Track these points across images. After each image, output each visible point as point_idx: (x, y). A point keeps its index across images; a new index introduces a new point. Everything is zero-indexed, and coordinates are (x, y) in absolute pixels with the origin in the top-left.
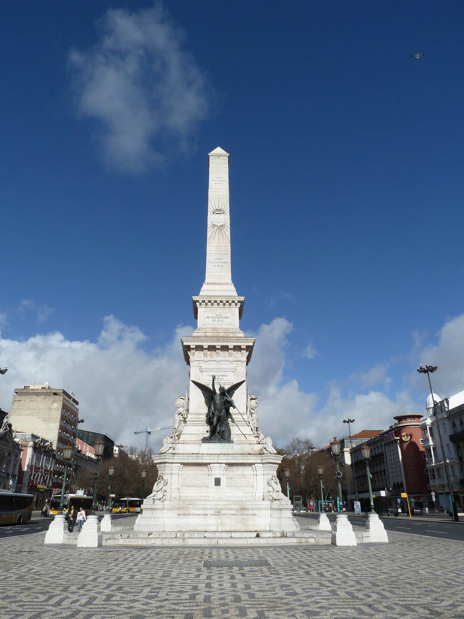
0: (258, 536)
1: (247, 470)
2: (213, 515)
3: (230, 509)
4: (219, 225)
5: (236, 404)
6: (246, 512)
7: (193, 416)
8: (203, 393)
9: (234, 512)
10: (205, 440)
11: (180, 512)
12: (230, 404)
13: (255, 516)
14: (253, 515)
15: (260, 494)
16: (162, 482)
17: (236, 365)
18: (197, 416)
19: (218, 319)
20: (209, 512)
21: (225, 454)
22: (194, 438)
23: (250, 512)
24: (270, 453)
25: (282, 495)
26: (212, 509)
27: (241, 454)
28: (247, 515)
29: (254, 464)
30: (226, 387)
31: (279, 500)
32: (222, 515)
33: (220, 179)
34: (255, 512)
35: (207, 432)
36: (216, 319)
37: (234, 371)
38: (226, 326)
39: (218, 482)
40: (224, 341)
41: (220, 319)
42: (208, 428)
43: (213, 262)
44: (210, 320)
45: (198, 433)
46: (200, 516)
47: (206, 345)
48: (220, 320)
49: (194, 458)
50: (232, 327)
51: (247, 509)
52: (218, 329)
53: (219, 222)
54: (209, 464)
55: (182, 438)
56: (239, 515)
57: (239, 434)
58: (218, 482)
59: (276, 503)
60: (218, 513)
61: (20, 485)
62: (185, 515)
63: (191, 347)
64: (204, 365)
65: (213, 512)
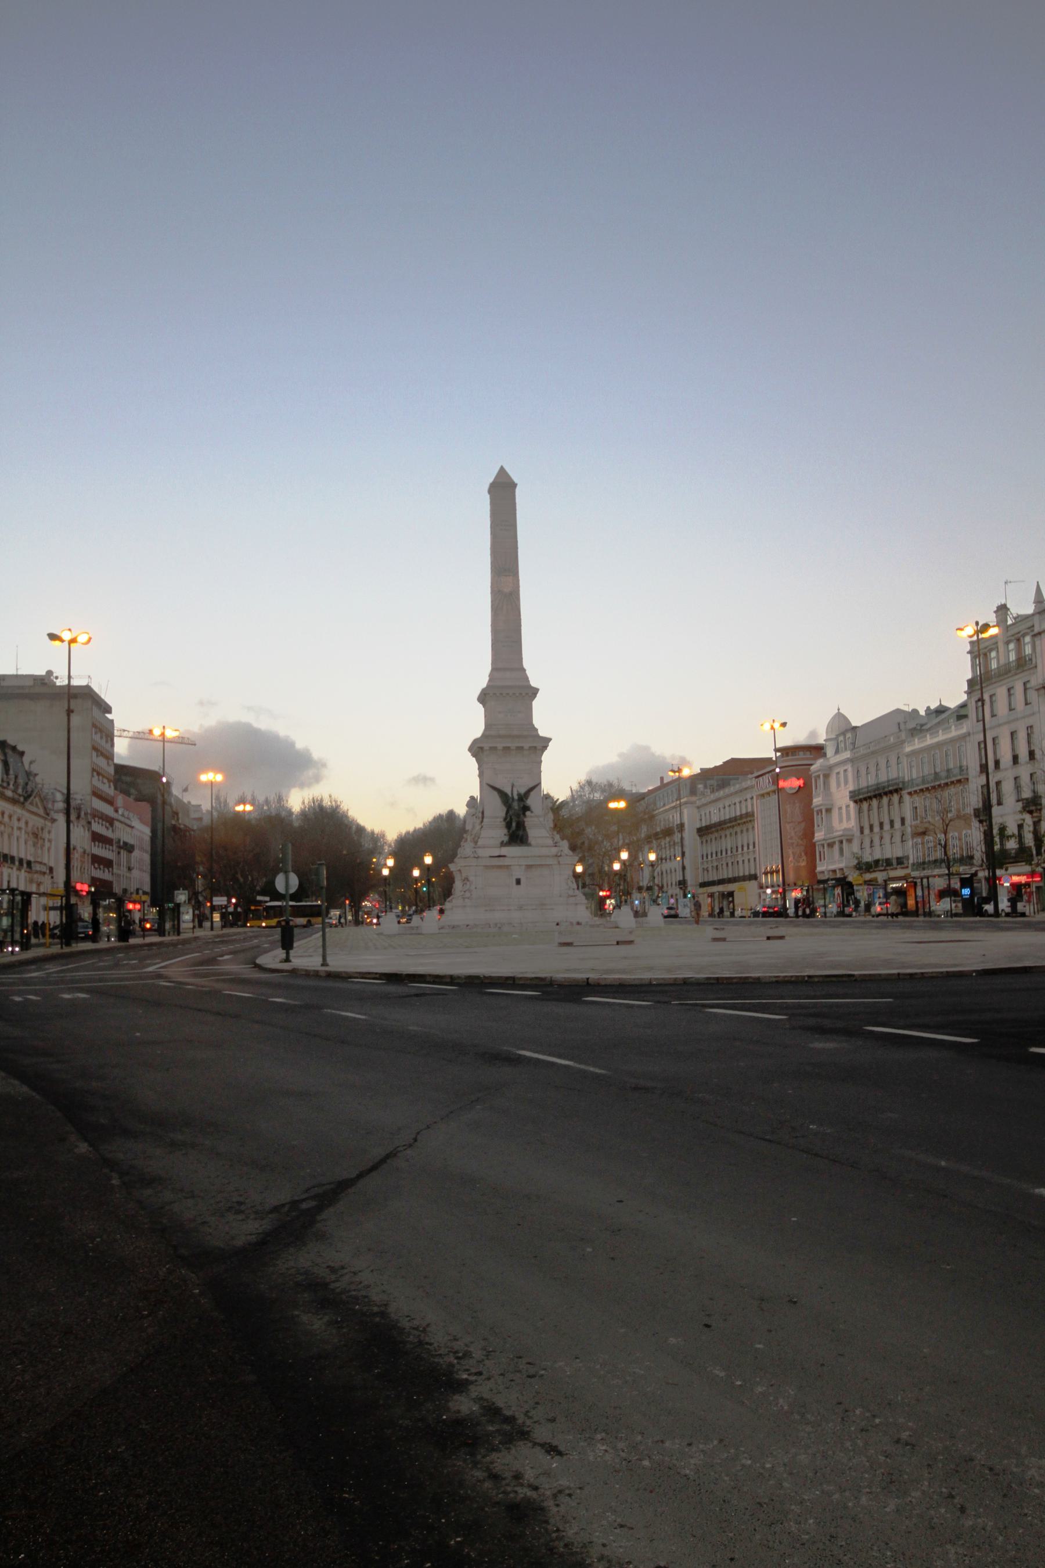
0: (558, 924)
4: (507, 590)
5: (533, 807)
8: (498, 793)
10: (503, 844)
12: (526, 809)
16: (468, 883)
21: (524, 857)
24: (567, 855)
25: (577, 892)
30: (523, 791)
35: (505, 835)
39: (518, 882)
42: (505, 831)
47: (500, 746)
55: (480, 843)
58: (518, 882)
59: (572, 900)
60: (520, 908)
63: (485, 748)
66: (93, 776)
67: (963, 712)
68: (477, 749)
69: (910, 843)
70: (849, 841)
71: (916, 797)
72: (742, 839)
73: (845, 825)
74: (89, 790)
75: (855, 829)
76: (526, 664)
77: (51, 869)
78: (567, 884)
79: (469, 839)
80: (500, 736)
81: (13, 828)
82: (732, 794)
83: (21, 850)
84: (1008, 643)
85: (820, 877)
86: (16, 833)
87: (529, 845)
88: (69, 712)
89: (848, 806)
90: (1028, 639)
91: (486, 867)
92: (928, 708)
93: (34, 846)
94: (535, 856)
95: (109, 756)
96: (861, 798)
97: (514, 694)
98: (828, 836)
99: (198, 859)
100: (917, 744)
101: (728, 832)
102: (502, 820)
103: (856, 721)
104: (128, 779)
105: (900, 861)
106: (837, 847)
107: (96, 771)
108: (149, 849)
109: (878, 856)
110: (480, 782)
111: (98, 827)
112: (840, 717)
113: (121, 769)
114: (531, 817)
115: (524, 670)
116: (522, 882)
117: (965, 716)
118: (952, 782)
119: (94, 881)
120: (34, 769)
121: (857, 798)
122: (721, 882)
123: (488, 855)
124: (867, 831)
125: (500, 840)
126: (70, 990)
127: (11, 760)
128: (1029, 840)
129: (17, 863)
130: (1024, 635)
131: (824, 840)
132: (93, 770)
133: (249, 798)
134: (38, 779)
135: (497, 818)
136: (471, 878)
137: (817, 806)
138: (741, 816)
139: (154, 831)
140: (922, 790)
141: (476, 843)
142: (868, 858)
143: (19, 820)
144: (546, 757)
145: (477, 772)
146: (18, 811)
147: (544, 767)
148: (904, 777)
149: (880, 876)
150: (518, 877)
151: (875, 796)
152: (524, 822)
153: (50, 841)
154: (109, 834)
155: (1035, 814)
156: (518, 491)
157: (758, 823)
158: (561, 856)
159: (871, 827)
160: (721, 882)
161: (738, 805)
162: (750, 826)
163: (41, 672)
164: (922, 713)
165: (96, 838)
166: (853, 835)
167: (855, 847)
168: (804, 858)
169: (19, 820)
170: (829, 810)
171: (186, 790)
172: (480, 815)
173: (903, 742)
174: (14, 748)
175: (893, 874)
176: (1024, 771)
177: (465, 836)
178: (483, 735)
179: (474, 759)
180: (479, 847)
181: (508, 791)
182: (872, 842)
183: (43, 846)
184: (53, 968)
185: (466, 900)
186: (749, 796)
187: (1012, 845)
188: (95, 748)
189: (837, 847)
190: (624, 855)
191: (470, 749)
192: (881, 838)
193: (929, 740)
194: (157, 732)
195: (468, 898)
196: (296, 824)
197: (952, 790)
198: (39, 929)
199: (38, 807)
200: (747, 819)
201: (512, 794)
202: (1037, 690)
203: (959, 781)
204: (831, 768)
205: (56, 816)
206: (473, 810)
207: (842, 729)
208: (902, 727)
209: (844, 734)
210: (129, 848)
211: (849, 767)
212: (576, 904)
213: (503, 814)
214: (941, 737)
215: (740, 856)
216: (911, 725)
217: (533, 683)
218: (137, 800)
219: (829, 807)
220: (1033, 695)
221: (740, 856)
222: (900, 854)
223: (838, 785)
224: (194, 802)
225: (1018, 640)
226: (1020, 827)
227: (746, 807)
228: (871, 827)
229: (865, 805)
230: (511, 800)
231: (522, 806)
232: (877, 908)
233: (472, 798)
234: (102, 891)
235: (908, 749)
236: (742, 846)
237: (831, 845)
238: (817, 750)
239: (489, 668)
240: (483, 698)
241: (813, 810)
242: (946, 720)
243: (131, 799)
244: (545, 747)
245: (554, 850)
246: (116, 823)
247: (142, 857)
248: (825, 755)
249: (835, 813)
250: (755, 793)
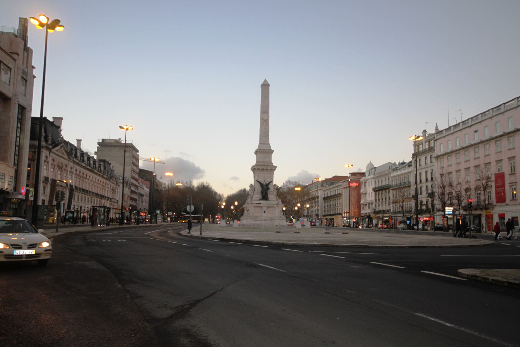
0: (277, 226)
1: (273, 209)
4: (265, 118)
9: (269, 220)
11: (254, 220)
12: (268, 188)
15: (276, 215)
16: (249, 212)
20: (262, 220)
22: (257, 199)
25: (283, 216)
30: (267, 183)
31: (282, 217)
39: (265, 212)
42: (261, 195)
47: (261, 168)
51: (273, 219)
58: (265, 212)
59: (281, 218)
60: (265, 220)
66: (132, 172)
67: (410, 164)
68: (254, 169)
69: (391, 205)
70: (372, 204)
71: (394, 191)
72: (337, 202)
73: (371, 199)
74: (130, 176)
75: (374, 200)
76: (270, 142)
77: (117, 201)
78: (280, 213)
79: (249, 197)
80: (261, 165)
81: (106, 187)
82: (335, 187)
83: (108, 194)
84: (426, 142)
85: (362, 215)
86: (107, 189)
88: (125, 151)
89: (372, 193)
90: (432, 141)
91: (255, 207)
92: (399, 162)
93: (113, 193)
94: (270, 204)
95: (137, 166)
96: (376, 190)
97: (266, 152)
98: (365, 202)
99: (164, 200)
100: (395, 174)
101: (333, 199)
102: (260, 192)
103: (376, 166)
104: (143, 174)
105: (388, 211)
106: (367, 206)
107: (133, 171)
108: (148, 196)
109: (381, 209)
110: (254, 179)
111: (132, 188)
112: (370, 164)
113: (141, 170)
114: (270, 191)
115: (269, 144)
116: (266, 212)
117: (411, 165)
118: (406, 187)
119: (131, 205)
120: (114, 169)
121: (375, 190)
122: (330, 215)
123: (255, 203)
124: (377, 201)
125: (260, 198)
126: (121, 239)
127: (106, 166)
128: (430, 206)
129: (107, 199)
130: (431, 140)
131: (364, 203)
132: (132, 170)
133: (181, 181)
134: (115, 172)
136: (249, 210)
137: (362, 192)
138: (337, 194)
139: (150, 190)
140: (396, 189)
141: (252, 199)
142: (377, 210)
143: (108, 185)
144: (275, 172)
145: (253, 176)
146: (108, 182)
147: (274, 175)
148: (390, 184)
149: (381, 216)
150: (265, 210)
151: (381, 190)
152: (267, 193)
153: (117, 192)
154: (136, 191)
155: (432, 198)
156: (270, 87)
157: (343, 197)
158: (278, 204)
159: (379, 200)
160: (330, 215)
161: (336, 191)
162: (340, 198)
163: (117, 138)
164: (397, 164)
165: (132, 192)
166: (373, 202)
167: (374, 206)
168: (357, 208)
169: (108, 185)
170: (366, 194)
171: (161, 178)
172: (253, 190)
173: (390, 173)
174: (108, 162)
175: (385, 215)
176: (429, 184)
177: (248, 196)
179: (252, 172)
180: (253, 200)
181: (263, 183)
182: (379, 204)
183: (115, 193)
184: (116, 232)
185: (248, 217)
186: (340, 188)
187: (424, 207)
188: (133, 163)
189: (367, 206)
190: (299, 205)
191: (251, 169)
192: (382, 203)
193: (399, 173)
194: (152, 159)
195: (248, 216)
196: (195, 190)
197: (406, 189)
198: (112, 220)
200: (339, 195)
201: (264, 183)
202: (435, 158)
203: (408, 186)
204: (367, 180)
205: (120, 184)
206: (251, 188)
207: (372, 169)
208: (391, 168)
209: (372, 169)
210: (142, 195)
211: (373, 180)
212: (283, 220)
214: (403, 171)
215: (336, 207)
216: (394, 167)
217: (272, 149)
218: (145, 180)
219: (365, 193)
220: (433, 160)
221: (336, 207)
222: (388, 209)
223: (369, 186)
224: (163, 182)
225: (429, 142)
226: (427, 202)
227: (339, 191)
228: (379, 200)
229: (377, 193)
230: (263, 186)
231: (267, 188)
232: (380, 226)
233: (251, 184)
234: (133, 208)
235: (392, 175)
236: (337, 204)
237: (366, 205)
238: (363, 174)
239: (258, 143)
240: (256, 153)
241: (360, 193)
242: (405, 166)
243: (143, 180)
244: (275, 169)
245: (276, 202)
246: (139, 187)
247: (146, 198)
248: (365, 176)
249: (368, 195)
250: (342, 187)
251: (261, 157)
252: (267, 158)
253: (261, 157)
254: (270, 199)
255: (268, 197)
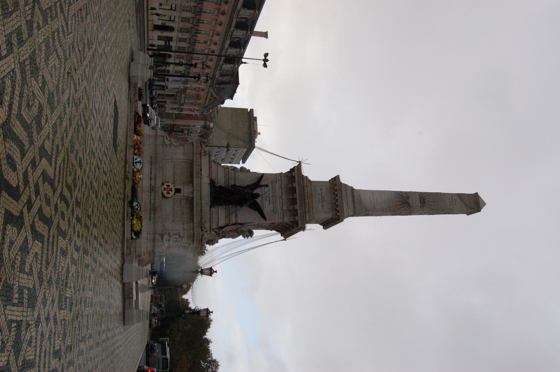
2: (151, 184)
3: (155, 199)
6: (152, 212)
7: (233, 175)
9: (152, 202)
11: (153, 159)
13: (149, 220)
14: (150, 218)
17: (279, 212)
18: (233, 178)
19: (321, 198)
20: (153, 181)
23: (152, 216)
26: (155, 183)
27: (201, 211)
28: (150, 213)
29: (193, 222)
32: (151, 193)
33: (454, 203)
34: (152, 220)
36: (320, 197)
37: (274, 211)
38: (314, 206)
40: (300, 200)
41: (321, 200)
43: (373, 196)
44: (319, 191)
45: (219, 179)
46: (150, 174)
47: (296, 185)
48: (320, 200)
49: (197, 170)
50: (315, 211)
51: (155, 214)
52: (312, 198)
53: (412, 201)
54: (193, 184)
56: (150, 206)
57: (218, 213)
58: (178, 191)
61: (174, 117)
62: (151, 162)
64: (278, 185)
65: (153, 185)
87: (211, 207)
91: (191, 164)
135: (235, 181)
150: (182, 192)
178: (303, 176)
199: (211, 99)
213: (237, 184)
251: (321, 189)
252: (323, 206)
253: (321, 189)
254: (213, 209)
255: (221, 205)
